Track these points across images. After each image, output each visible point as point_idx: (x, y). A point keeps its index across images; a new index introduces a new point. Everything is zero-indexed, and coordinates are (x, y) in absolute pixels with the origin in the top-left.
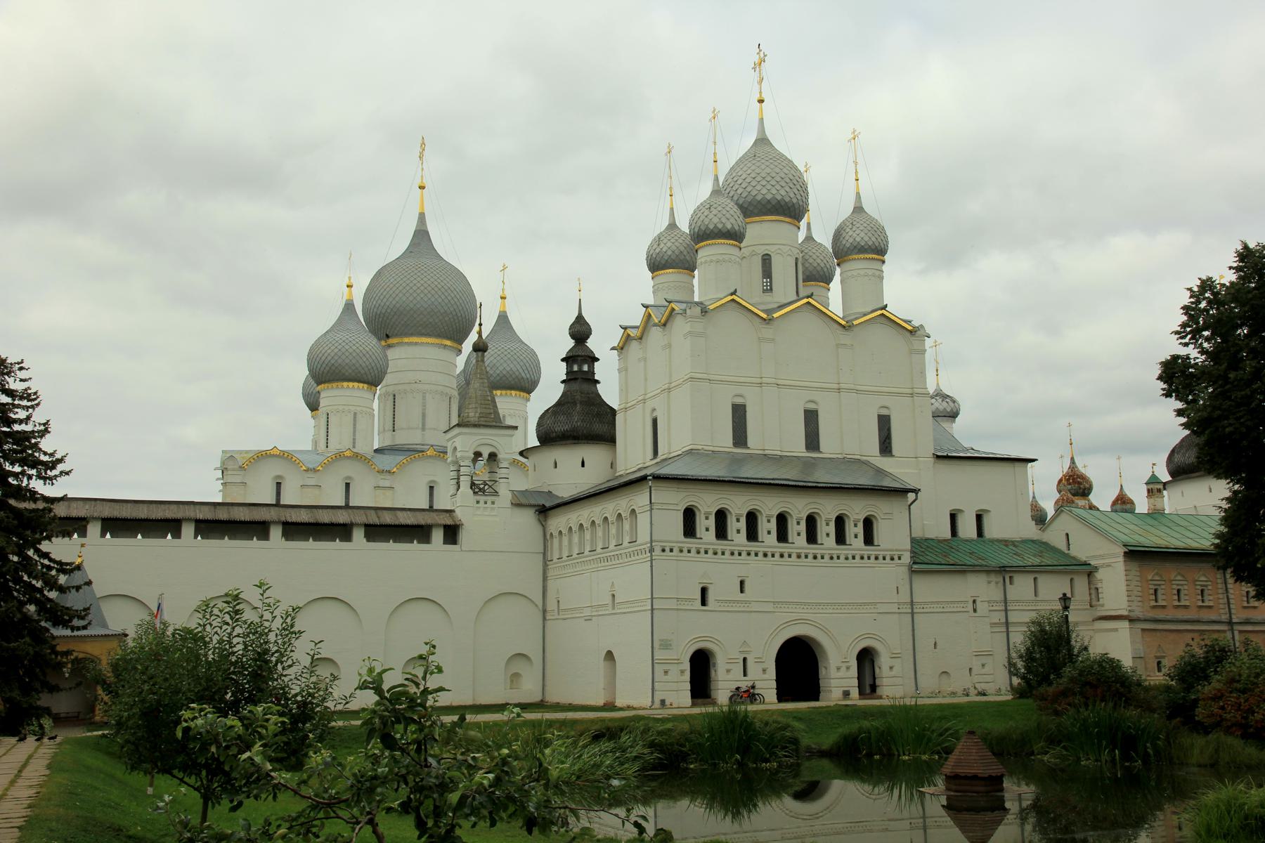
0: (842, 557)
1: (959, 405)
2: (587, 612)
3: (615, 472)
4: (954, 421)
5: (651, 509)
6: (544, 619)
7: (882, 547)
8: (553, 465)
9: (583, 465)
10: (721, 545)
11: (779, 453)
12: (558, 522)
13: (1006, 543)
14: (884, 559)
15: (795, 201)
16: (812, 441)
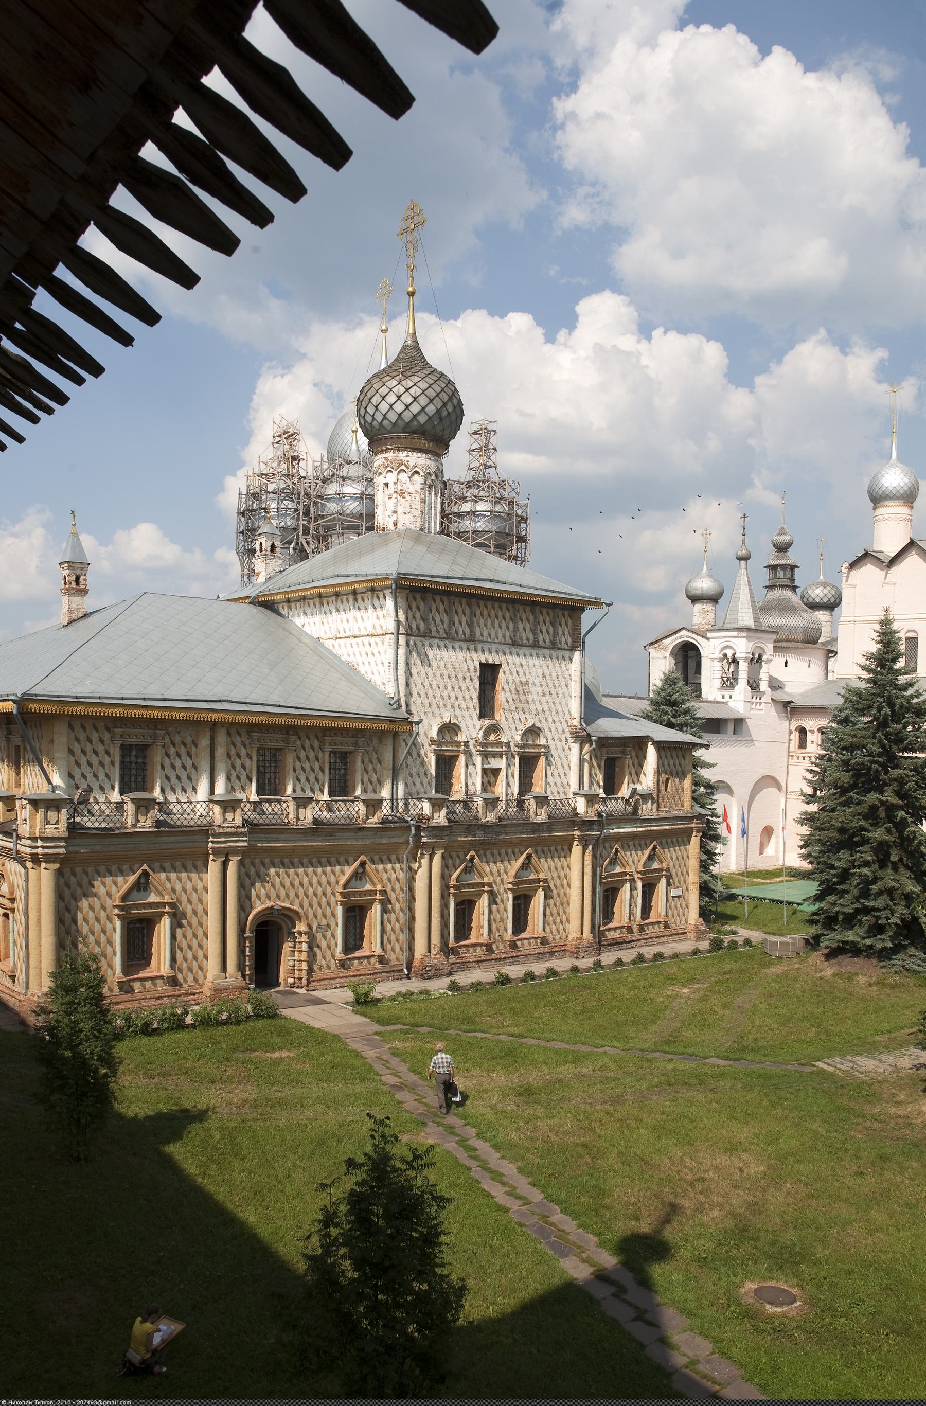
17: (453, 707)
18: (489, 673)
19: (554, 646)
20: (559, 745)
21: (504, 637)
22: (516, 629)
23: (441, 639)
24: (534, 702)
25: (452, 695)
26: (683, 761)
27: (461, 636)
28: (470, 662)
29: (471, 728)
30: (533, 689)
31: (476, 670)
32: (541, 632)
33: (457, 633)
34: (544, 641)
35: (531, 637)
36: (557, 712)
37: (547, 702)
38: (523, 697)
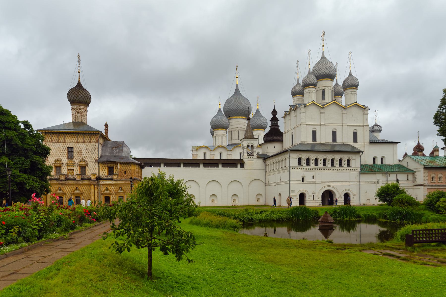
0: (341, 170)
1: (382, 128)
2: (275, 184)
3: (283, 149)
4: (380, 133)
5: (290, 158)
6: (265, 186)
7: (352, 167)
8: (267, 148)
9: (275, 148)
10: (308, 167)
11: (325, 143)
12: (269, 162)
13: (389, 165)
14: (353, 170)
15: (332, 74)
16: (334, 139)
17: (59, 156)
18: (70, 150)
19: (90, 142)
20: (92, 164)
21: (74, 141)
22: (78, 139)
23: (55, 142)
24: (83, 155)
25: (59, 154)
26: (130, 167)
27: (62, 142)
28: (64, 147)
29: (65, 161)
30: (83, 152)
31: (65, 148)
32: (86, 139)
33: (60, 141)
34: (87, 141)
35: (83, 141)
36: (91, 157)
37: (88, 155)
38: (80, 154)
